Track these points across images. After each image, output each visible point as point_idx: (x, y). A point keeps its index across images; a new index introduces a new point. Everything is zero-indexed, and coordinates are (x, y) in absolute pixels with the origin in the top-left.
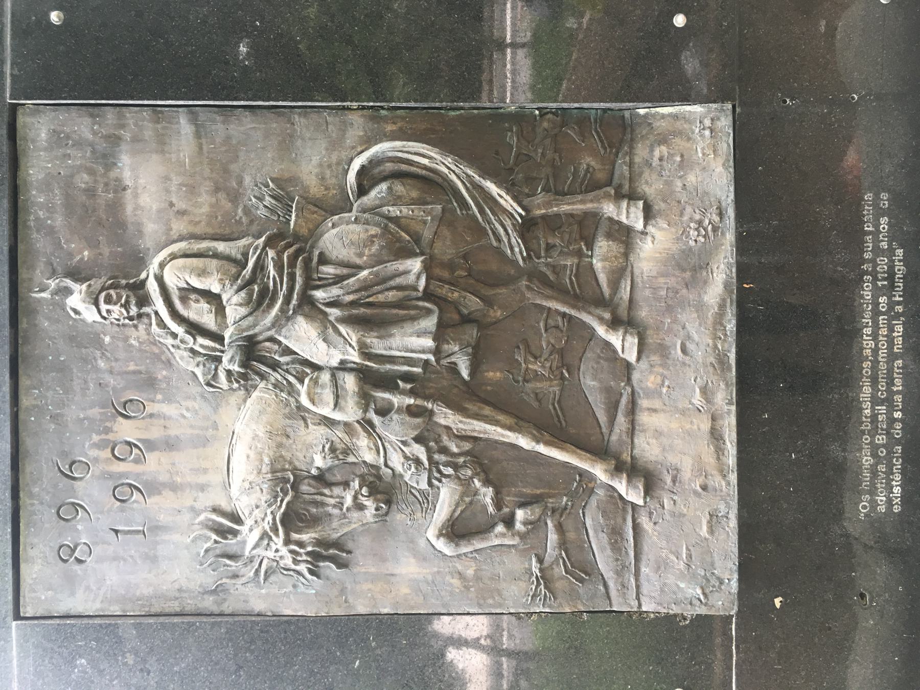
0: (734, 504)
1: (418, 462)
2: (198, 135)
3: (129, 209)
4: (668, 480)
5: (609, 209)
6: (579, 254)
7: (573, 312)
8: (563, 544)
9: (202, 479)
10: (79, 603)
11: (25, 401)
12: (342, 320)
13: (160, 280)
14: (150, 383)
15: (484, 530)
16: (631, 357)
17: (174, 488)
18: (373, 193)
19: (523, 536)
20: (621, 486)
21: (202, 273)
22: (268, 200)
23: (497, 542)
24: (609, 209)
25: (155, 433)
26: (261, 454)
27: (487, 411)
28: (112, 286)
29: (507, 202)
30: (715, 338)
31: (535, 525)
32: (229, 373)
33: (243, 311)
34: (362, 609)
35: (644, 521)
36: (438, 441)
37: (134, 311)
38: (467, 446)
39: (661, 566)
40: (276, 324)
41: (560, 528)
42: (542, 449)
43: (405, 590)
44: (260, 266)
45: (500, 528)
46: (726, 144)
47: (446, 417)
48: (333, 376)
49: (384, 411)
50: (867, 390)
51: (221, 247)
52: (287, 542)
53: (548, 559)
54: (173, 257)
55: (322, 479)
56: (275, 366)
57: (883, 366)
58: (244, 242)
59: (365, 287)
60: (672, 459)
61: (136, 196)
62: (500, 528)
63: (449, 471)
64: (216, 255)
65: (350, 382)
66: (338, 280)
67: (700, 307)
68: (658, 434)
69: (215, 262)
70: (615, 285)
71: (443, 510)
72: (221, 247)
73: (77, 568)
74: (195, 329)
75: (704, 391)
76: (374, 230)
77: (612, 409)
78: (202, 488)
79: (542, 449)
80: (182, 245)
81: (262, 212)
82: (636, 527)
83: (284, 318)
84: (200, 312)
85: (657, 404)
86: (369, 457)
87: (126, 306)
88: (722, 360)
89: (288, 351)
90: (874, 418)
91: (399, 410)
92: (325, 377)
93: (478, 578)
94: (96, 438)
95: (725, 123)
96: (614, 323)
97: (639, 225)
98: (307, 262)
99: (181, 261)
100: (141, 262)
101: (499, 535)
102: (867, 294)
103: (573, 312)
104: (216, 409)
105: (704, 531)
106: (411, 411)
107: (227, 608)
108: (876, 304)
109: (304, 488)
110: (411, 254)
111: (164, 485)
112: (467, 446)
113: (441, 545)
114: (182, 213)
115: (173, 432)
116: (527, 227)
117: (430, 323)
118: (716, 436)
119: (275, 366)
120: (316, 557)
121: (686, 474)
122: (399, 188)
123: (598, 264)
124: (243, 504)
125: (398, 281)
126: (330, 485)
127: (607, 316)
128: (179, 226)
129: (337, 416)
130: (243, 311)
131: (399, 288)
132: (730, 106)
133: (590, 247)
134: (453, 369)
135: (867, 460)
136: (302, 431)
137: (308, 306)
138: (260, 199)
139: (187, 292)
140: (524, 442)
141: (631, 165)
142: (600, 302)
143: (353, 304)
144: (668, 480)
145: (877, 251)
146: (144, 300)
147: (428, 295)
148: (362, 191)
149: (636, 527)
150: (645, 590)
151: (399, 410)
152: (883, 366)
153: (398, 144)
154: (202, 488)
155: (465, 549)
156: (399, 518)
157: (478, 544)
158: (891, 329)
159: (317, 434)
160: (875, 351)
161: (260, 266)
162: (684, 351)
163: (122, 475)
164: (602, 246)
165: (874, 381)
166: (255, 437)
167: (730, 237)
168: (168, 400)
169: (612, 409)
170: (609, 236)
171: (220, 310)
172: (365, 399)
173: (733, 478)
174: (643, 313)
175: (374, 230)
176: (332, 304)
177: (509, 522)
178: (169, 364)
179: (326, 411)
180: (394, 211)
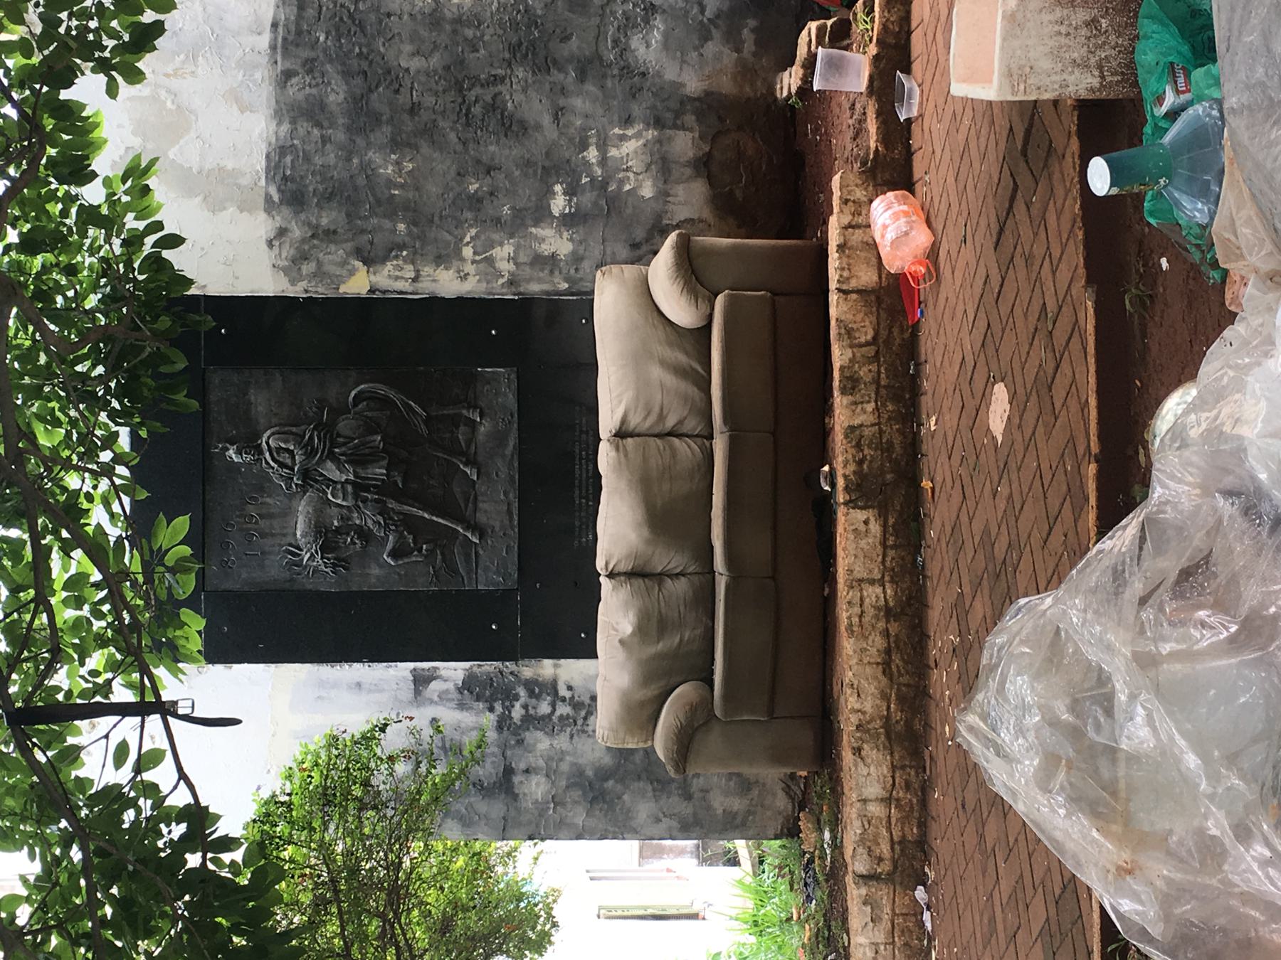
0: (517, 541)
1: (380, 523)
2: (283, 380)
3: (253, 412)
4: (490, 531)
5: (465, 412)
6: (452, 432)
7: (449, 458)
8: (444, 560)
9: (285, 531)
10: (229, 585)
11: (208, 497)
12: (346, 462)
13: (267, 443)
14: (261, 489)
15: (409, 554)
16: (475, 478)
17: (273, 535)
18: (360, 406)
19: (426, 557)
20: (469, 535)
21: (286, 442)
22: (314, 409)
23: (414, 559)
24: (465, 412)
25: (264, 511)
26: (310, 520)
27: (410, 501)
28: (248, 447)
29: (419, 410)
30: (509, 469)
31: (431, 552)
32: (296, 485)
33: (303, 457)
34: (354, 589)
35: (481, 552)
36: (388, 514)
37: (256, 457)
38: (401, 517)
39: (486, 569)
40: (318, 463)
41: (442, 554)
42: (435, 518)
43: (373, 580)
44: (311, 438)
45: (416, 553)
46: (514, 386)
47: (392, 504)
48: (342, 487)
49: (365, 501)
50: (577, 492)
51: (294, 429)
52: (322, 558)
53: (437, 567)
54: (273, 434)
55: (338, 531)
56: (316, 481)
57: (584, 482)
58: (303, 427)
59: (356, 447)
60: (492, 522)
61: (256, 407)
62: (416, 553)
63: (393, 528)
64: (292, 433)
65: (350, 488)
66: (344, 444)
67: (504, 456)
68: (486, 511)
69: (292, 437)
70: (468, 446)
71: (390, 546)
72: (294, 429)
73: (229, 570)
74: (282, 465)
75: (506, 494)
76: (362, 423)
77: (467, 501)
78: (284, 535)
79: (435, 518)
80: (277, 428)
81: (311, 414)
82: (476, 553)
83: (321, 461)
84: (284, 458)
85: (485, 499)
86: (358, 522)
87: (253, 455)
88: (512, 478)
89: (322, 475)
90: (580, 503)
91: (371, 501)
92: (339, 486)
93: (406, 575)
94: (238, 513)
95: (513, 376)
96: (466, 464)
97: (478, 419)
98: (331, 436)
99: (277, 436)
100: (260, 437)
101: (415, 558)
102: (577, 451)
103: (449, 458)
104: (290, 500)
105: (504, 554)
106: (376, 501)
107: (295, 588)
108: (581, 454)
109: (330, 535)
110: (377, 433)
111: (267, 534)
112: (401, 517)
113: (389, 560)
114: (276, 414)
115: (272, 510)
116: (428, 421)
117: (385, 463)
118: (509, 512)
119: (316, 481)
120: (334, 566)
121: (497, 529)
122: (372, 405)
123: (460, 437)
124: (302, 542)
125: (372, 445)
126: (340, 534)
127: (464, 459)
128: (274, 420)
129: (344, 503)
130: (303, 457)
131: (372, 448)
132: (515, 369)
133: (457, 428)
134: (396, 483)
135: (577, 523)
136: (328, 510)
137: (332, 457)
138: (310, 408)
139: (279, 449)
140: (426, 515)
141: (475, 393)
142: (462, 453)
143: (351, 454)
144: (490, 531)
145: (581, 432)
146: (261, 452)
147: (384, 450)
148: (355, 404)
149: (476, 553)
150: (480, 579)
151: (371, 501)
152: (584, 482)
153: (371, 385)
154: (284, 535)
155: (400, 562)
156: (371, 549)
157: (406, 560)
158: (587, 466)
159: (335, 510)
160: (580, 475)
161: (311, 438)
162: (497, 475)
163: (251, 529)
164: (462, 428)
165: (580, 490)
166: (308, 512)
167: (516, 425)
168: (269, 496)
169: (467, 501)
170: (465, 425)
171: (293, 458)
172: (356, 496)
173: (516, 530)
174: (480, 459)
175: (362, 423)
176: (342, 455)
177: (420, 550)
178: (270, 480)
179: (339, 501)
180: (369, 414)
